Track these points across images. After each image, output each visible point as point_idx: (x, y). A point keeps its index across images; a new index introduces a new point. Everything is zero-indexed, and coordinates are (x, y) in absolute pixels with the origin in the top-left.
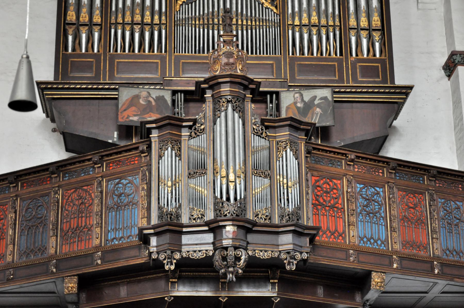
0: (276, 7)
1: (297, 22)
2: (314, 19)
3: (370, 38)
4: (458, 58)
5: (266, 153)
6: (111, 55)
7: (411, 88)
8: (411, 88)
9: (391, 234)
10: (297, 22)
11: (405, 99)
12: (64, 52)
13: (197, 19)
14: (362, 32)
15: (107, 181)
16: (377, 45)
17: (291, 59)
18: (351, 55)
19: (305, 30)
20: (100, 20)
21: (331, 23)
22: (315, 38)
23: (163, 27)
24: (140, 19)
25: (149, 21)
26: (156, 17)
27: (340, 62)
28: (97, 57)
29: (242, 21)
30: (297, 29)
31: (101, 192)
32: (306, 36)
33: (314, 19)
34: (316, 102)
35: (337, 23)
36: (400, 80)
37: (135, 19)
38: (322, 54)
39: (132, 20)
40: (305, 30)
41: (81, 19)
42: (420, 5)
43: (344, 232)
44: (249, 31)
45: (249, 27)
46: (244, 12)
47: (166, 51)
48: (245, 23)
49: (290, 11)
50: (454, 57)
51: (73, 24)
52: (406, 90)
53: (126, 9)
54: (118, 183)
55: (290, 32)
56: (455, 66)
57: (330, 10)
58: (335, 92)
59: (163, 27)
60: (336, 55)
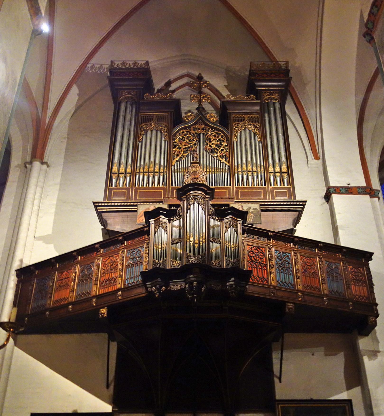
0: (228, 162)
1: (240, 170)
2: (250, 168)
3: (281, 176)
4: (332, 190)
5: (218, 228)
6: (136, 188)
7: (306, 202)
8: (306, 202)
9: (297, 280)
10: (240, 170)
11: (303, 208)
12: (110, 187)
13: (184, 169)
14: (276, 174)
15: (127, 251)
16: (286, 181)
17: (236, 188)
18: (271, 185)
19: (245, 173)
20: (130, 171)
21: (259, 170)
22: (250, 178)
24: (153, 170)
25: (158, 171)
26: (162, 168)
27: (264, 189)
28: (128, 189)
30: (240, 173)
31: (123, 257)
32: (245, 177)
33: (250, 168)
34: (251, 211)
35: (262, 170)
36: (299, 197)
37: (150, 170)
38: (254, 186)
39: (148, 171)
40: (245, 173)
41: (120, 170)
42: (309, 165)
43: (268, 278)
44: (213, 175)
45: (213, 173)
46: (211, 165)
47: (166, 185)
48: (211, 170)
49: (236, 164)
50: (330, 189)
51: (116, 173)
52: (303, 204)
53: (145, 165)
54: (133, 252)
55: (236, 175)
56: (331, 195)
57: (259, 163)
58: (261, 205)
60: (262, 185)
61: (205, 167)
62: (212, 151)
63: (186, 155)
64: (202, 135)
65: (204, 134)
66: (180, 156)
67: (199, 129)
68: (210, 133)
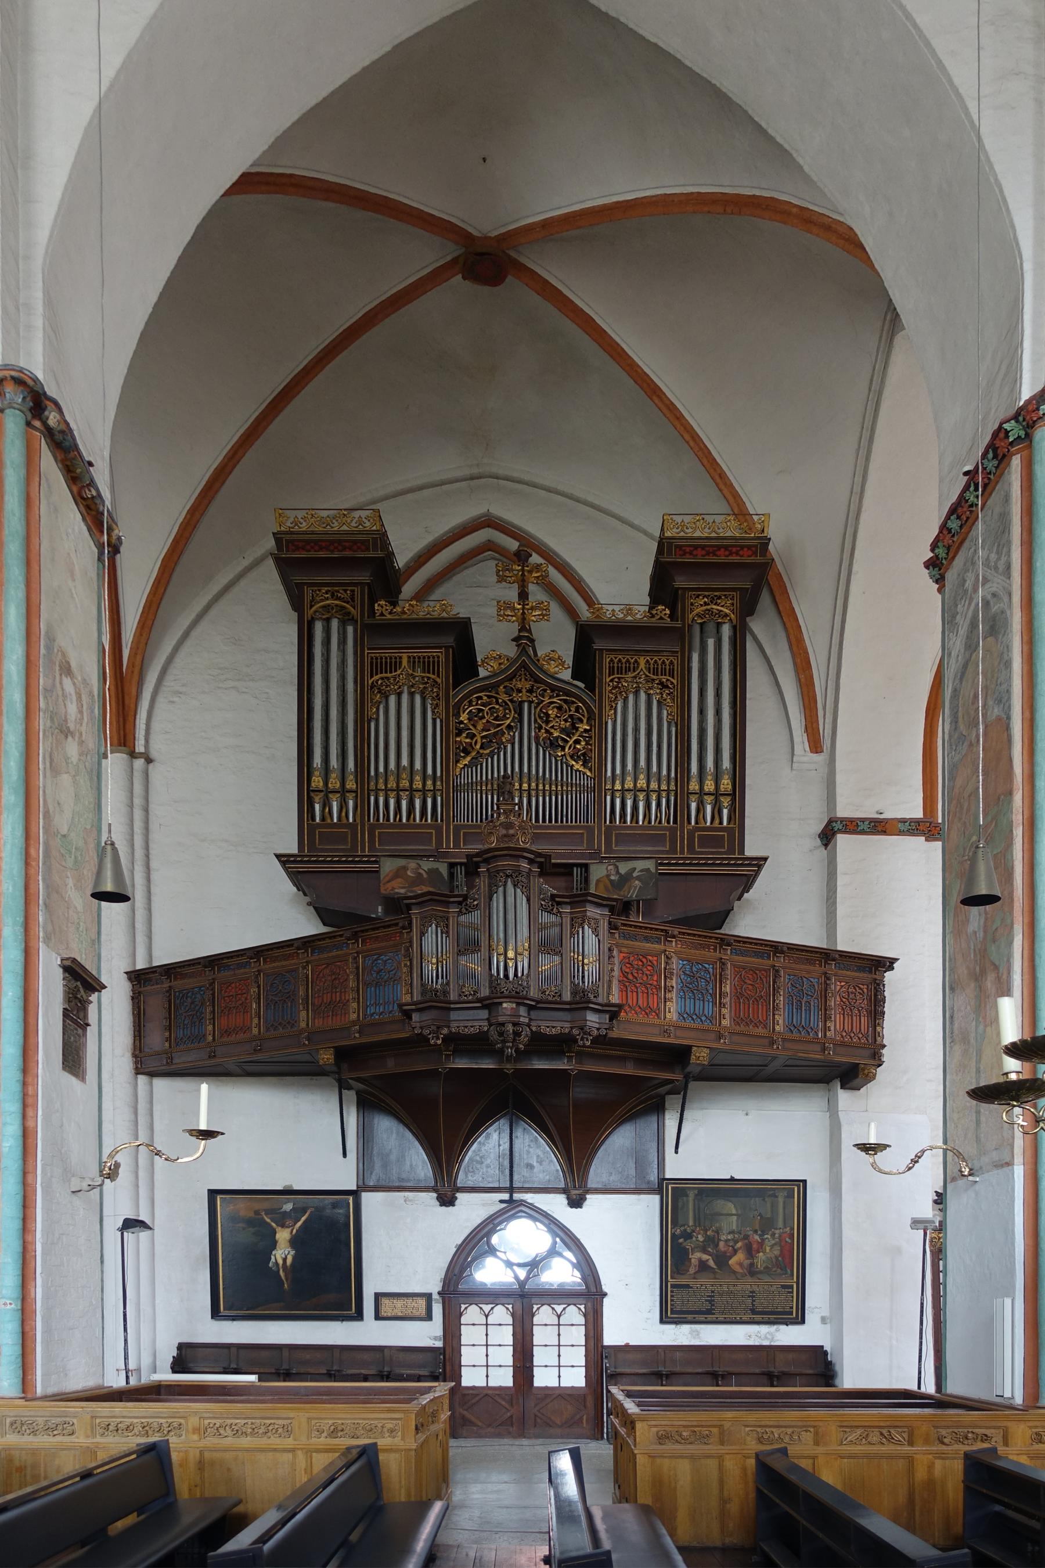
23: (439, 793)
29: (544, 786)
44: (554, 798)
48: (547, 787)
59: (439, 793)
61: (534, 779)
62: (552, 744)
63: (488, 751)
64: (526, 705)
65: (530, 702)
66: (474, 754)
67: (519, 691)
68: (547, 700)
